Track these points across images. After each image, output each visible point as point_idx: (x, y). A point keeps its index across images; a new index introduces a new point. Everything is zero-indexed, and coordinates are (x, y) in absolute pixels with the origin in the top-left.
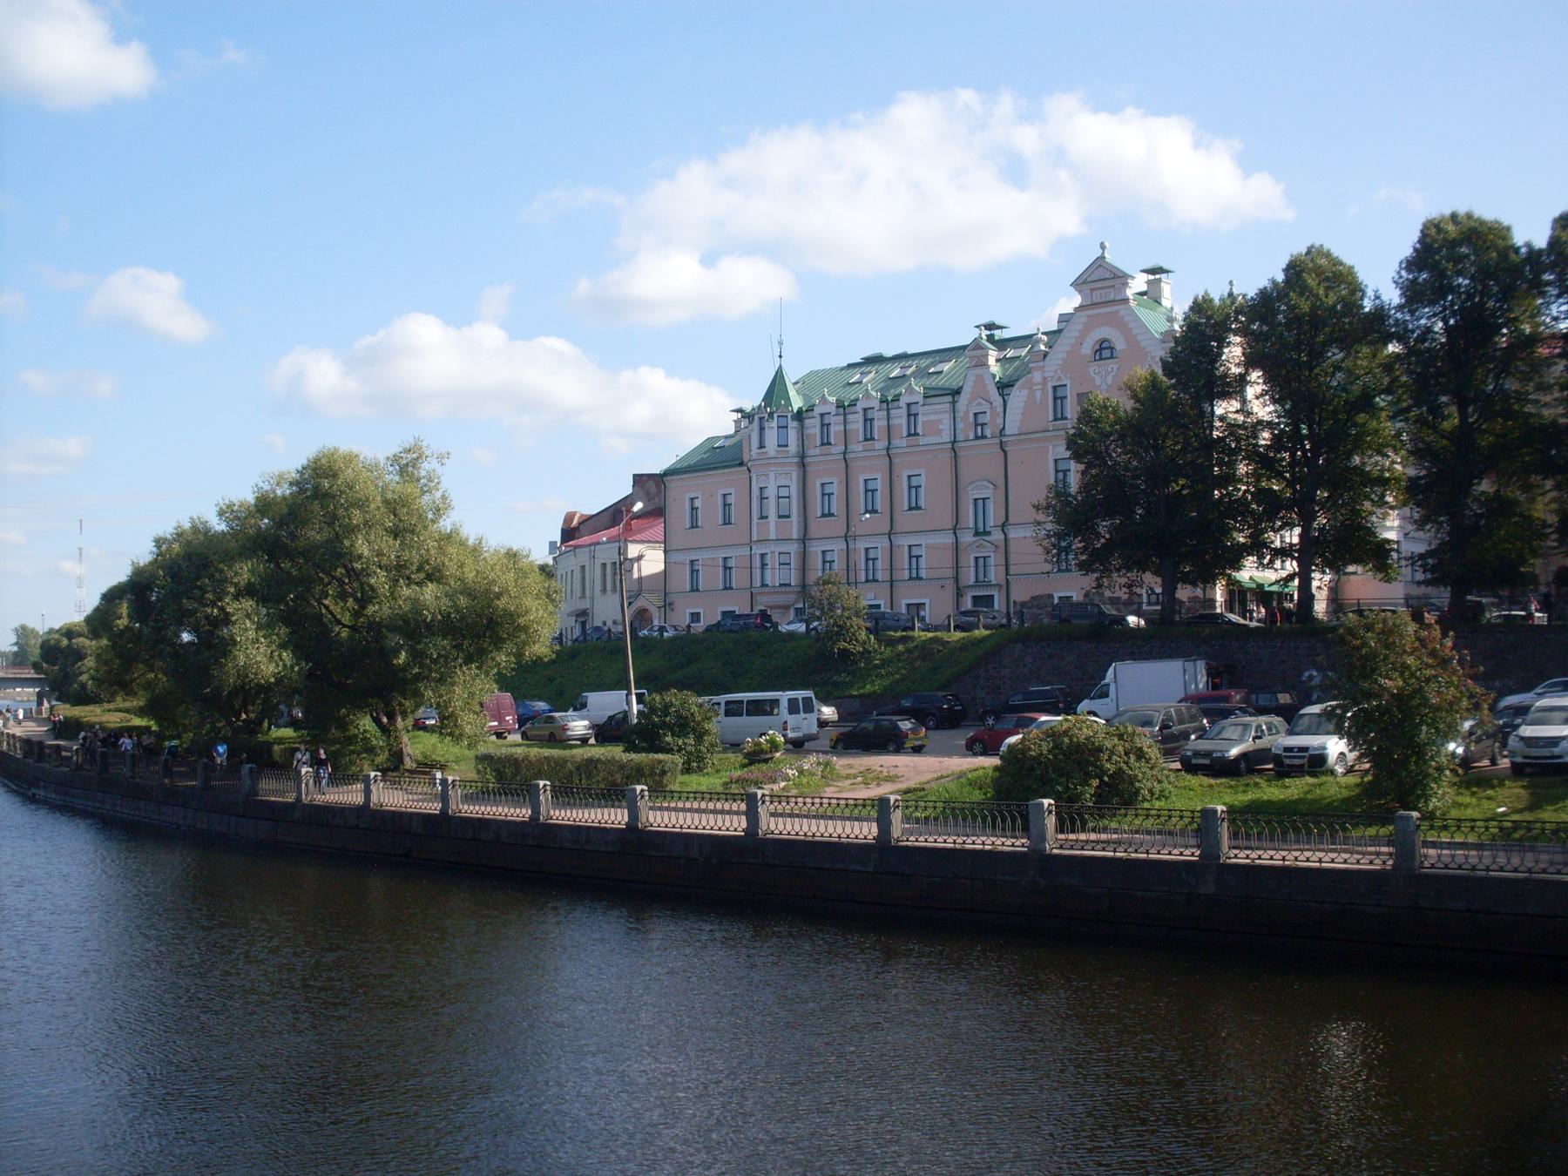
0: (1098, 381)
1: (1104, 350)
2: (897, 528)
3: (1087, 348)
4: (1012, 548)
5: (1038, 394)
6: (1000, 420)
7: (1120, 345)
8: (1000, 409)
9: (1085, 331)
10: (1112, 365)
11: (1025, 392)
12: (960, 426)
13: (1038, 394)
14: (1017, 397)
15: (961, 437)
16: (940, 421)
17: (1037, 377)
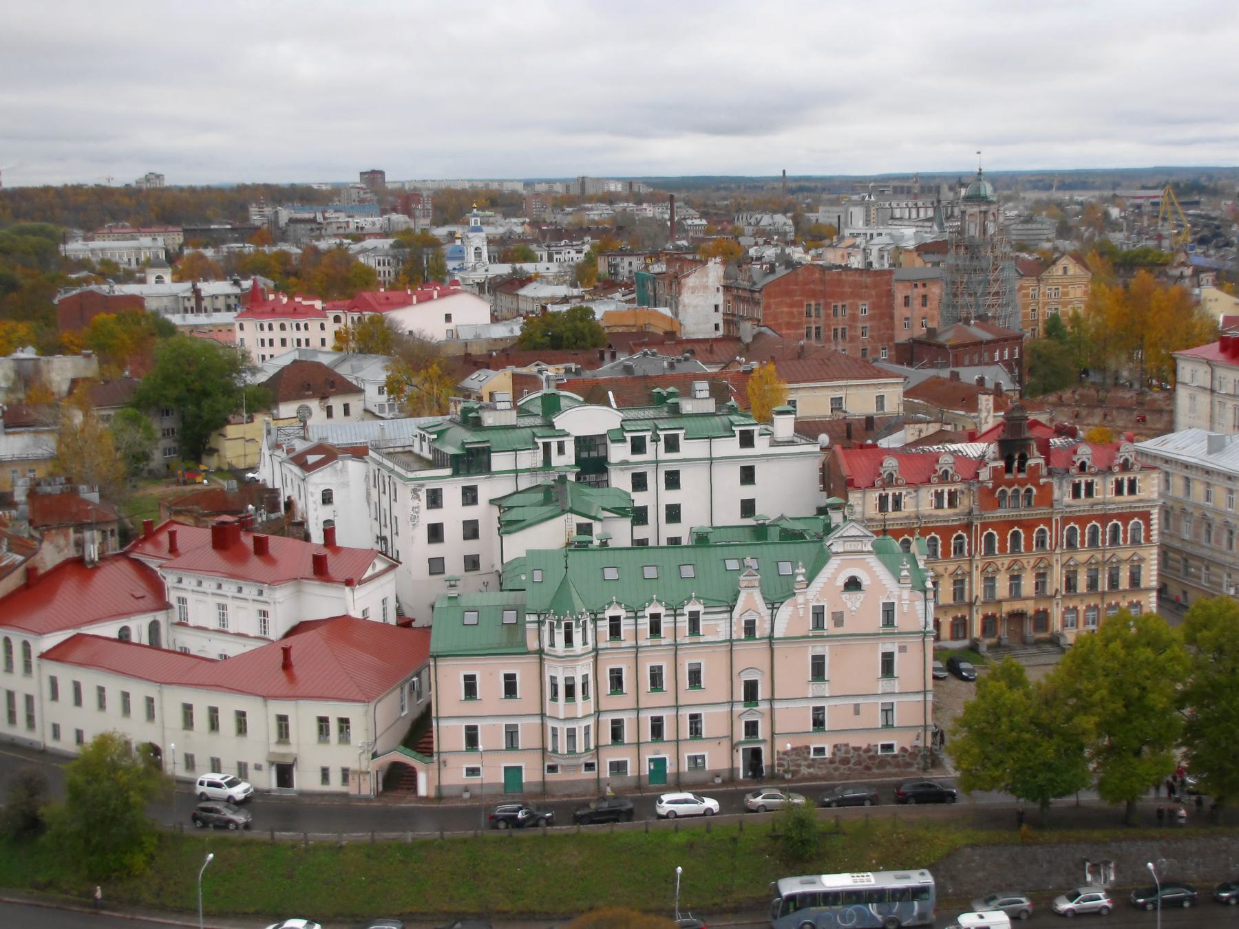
0: (849, 604)
1: (853, 584)
2: (680, 703)
3: (841, 580)
4: (777, 717)
5: (801, 612)
6: (767, 626)
7: (865, 580)
8: (768, 618)
9: (839, 569)
10: (859, 595)
11: (791, 609)
12: (734, 628)
13: (801, 612)
14: (785, 612)
15: (734, 637)
16: (717, 625)
17: (800, 599)
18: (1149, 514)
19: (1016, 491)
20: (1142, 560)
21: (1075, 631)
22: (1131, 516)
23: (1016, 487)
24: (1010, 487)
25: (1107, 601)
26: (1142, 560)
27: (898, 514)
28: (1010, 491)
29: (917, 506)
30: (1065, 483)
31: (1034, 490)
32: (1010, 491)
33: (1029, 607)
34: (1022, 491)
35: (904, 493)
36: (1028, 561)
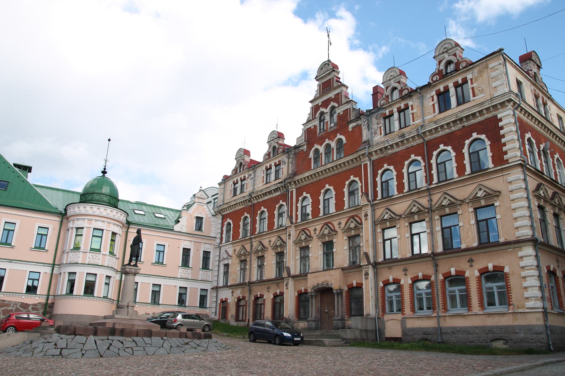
18: (496, 120)
19: (328, 146)
20: (493, 195)
21: (399, 316)
22: (466, 132)
23: (327, 141)
24: (321, 145)
25: (443, 269)
26: (493, 195)
27: (243, 195)
28: (322, 149)
29: (254, 185)
30: (374, 121)
31: (343, 138)
32: (322, 149)
33: (334, 279)
34: (333, 144)
35: (247, 176)
36: (340, 223)
